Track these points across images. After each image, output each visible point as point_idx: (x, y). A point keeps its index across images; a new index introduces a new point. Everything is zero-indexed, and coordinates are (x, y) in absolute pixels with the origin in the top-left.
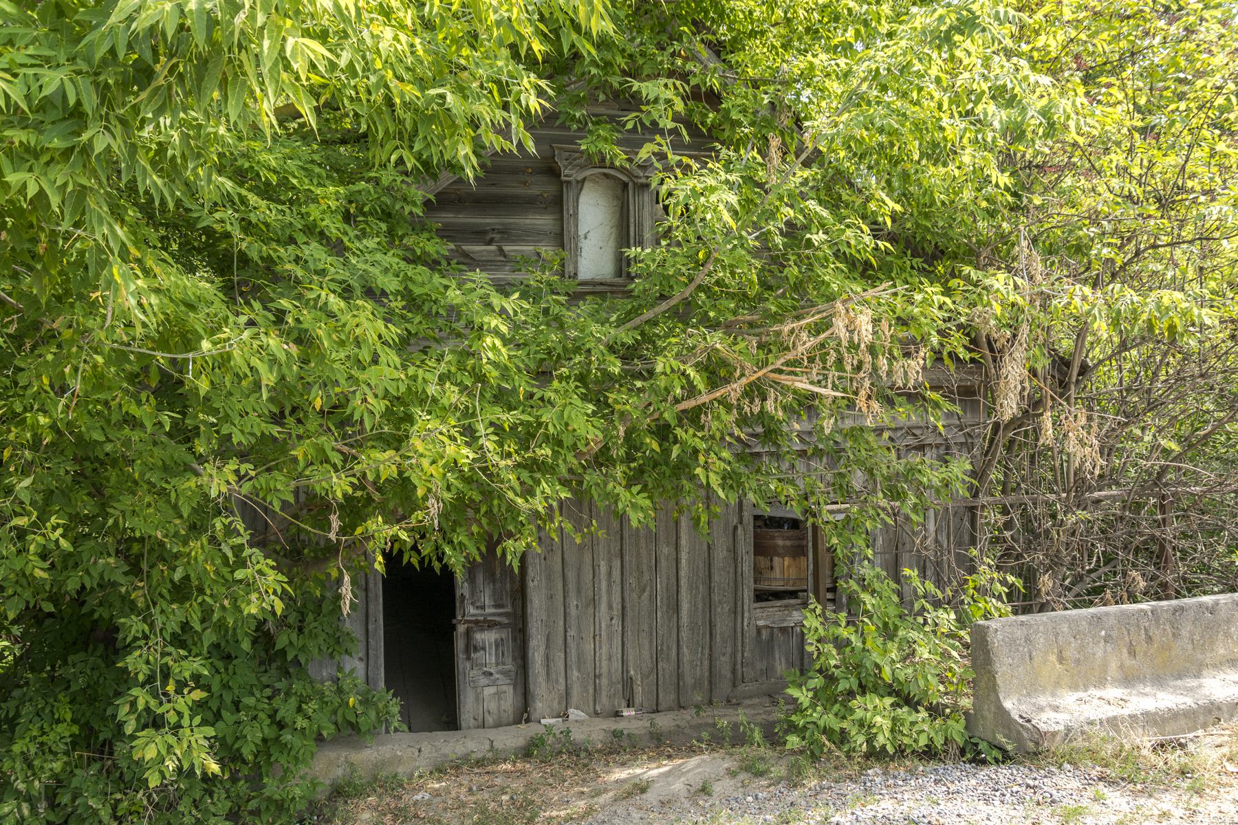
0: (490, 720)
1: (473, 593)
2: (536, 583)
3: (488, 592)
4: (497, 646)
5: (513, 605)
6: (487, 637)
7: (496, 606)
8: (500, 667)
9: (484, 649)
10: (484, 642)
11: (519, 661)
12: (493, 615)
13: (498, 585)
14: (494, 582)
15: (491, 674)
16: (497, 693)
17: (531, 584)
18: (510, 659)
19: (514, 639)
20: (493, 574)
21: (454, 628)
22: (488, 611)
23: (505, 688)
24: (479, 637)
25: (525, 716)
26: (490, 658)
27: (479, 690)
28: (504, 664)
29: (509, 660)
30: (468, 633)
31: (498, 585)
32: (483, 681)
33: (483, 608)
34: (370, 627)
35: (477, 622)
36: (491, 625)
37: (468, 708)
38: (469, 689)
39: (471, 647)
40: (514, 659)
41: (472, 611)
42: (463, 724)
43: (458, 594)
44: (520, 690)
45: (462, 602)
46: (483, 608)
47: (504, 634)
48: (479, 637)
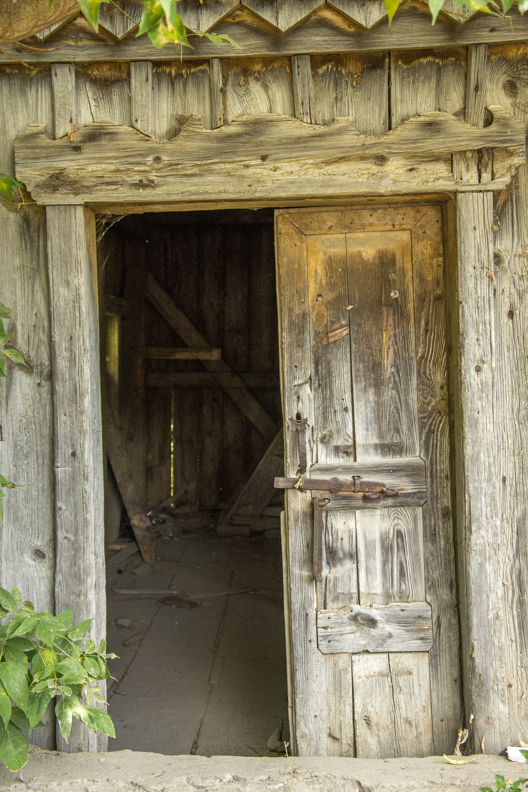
0: (369, 740)
1: (326, 410)
2: (486, 374)
3: (364, 409)
4: (387, 550)
5: (426, 446)
6: (362, 528)
7: (385, 448)
8: (396, 606)
9: (354, 556)
10: (353, 537)
11: (445, 594)
12: (377, 469)
13: (389, 393)
14: (378, 384)
15: (372, 622)
16: (390, 673)
17: (471, 379)
18: (420, 589)
19: (431, 536)
20: (376, 367)
21: (278, 499)
22: (367, 458)
23: (407, 661)
24: (343, 525)
25: (463, 735)
26: (367, 580)
27: (343, 661)
28: (404, 597)
29: (417, 588)
30: (313, 514)
31: (389, 393)
32: (353, 638)
34: (60, 472)
35: (335, 488)
36: (372, 497)
37: (314, 700)
38: (316, 657)
39: (321, 553)
40: (431, 586)
41: (326, 458)
42: (302, 745)
43: (289, 411)
44: (447, 661)
45: (299, 432)
46: (350, 451)
47: (408, 521)
48: (343, 525)
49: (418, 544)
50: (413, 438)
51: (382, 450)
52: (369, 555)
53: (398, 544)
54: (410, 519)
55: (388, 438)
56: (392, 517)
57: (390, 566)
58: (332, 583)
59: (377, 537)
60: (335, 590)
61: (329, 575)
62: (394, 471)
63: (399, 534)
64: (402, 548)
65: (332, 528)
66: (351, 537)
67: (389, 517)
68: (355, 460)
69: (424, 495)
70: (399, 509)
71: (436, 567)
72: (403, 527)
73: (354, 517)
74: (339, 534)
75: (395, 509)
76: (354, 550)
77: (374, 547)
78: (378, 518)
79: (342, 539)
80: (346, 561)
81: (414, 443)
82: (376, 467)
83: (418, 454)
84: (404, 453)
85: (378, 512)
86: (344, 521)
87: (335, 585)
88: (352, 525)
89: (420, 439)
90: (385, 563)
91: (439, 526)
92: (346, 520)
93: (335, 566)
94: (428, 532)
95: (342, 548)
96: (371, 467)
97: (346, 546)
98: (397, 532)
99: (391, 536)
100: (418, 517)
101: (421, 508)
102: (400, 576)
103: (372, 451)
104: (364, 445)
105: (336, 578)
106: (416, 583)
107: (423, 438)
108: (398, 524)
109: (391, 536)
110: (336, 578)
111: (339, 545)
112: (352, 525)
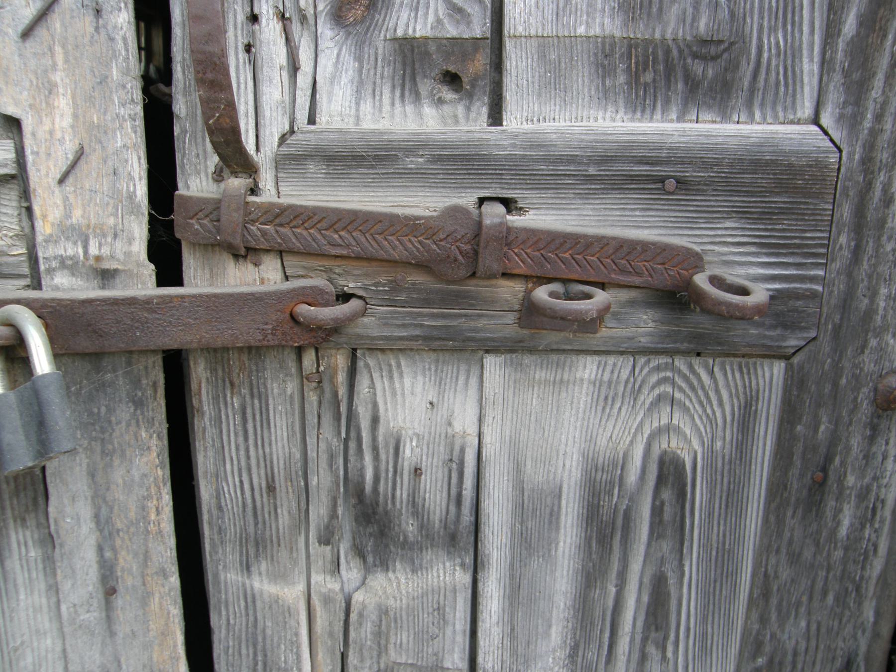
4: (604, 528)
7: (648, 70)
9: (463, 536)
33: (468, 68)
49: (741, 514)
50: (797, 25)
51: (634, 79)
52: (530, 540)
53: (657, 511)
54: (726, 408)
55: (673, 13)
56: (647, 397)
57: (613, 590)
58: (368, 627)
59: (569, 473)
60: (382, 650)
61: (358, 597)
62: (682, 183)
63: (670, 474)
64: (671, 524)
65: (375, 421)
66: (455, 464)
67: (636, 393)
68: (496, 117)
69: (812, 308)
70: (680, 363)
71: (799, 604)
72: (690, 442)
73: (474, 381)
74: (408, 452)
75: (663, 360)
76: (467, 517)
77: (554, 516)
78: (583, 396)
79: (417, 472)
80: (428, 555)
81: (796, 53)
82: (604, 160)
83: (806, 110)
84: (738, 100)
85: (588, 369)
86: (432, 395)
87: (380, 636)
88: (465, 421)
89: (831, 31)
90: (590, 577)
91: (848, 449)
92: (441, 393)
93: (384, 564)
94: (795, 471)
95: (416, 508)
96: (571, 160)
97: (435, 495)
98: (662, 463)
99: (632, 477)
100: (762, 406)
101: (778, 368)
102: (647, 627)
103: (582, 78)
104: (543, 44)
105: (383, 611)
106: (705, 649)
107: (850, 26)
108: (668, 429)
109: (632, 477)
110: (383, 611)
111: (402, 494)
112: (465, 421)
